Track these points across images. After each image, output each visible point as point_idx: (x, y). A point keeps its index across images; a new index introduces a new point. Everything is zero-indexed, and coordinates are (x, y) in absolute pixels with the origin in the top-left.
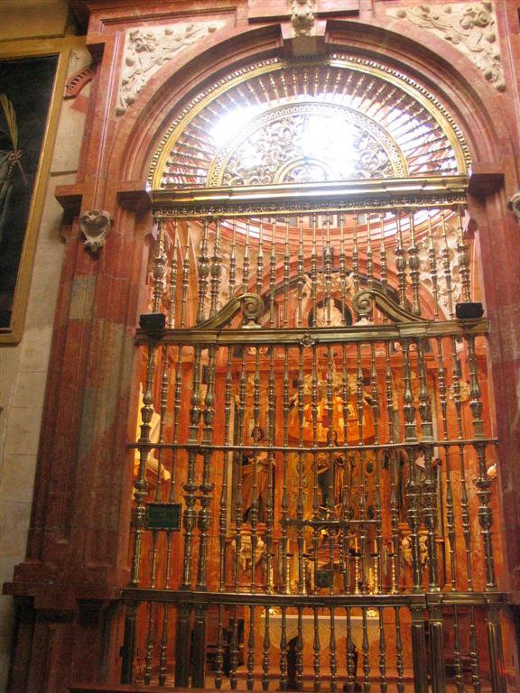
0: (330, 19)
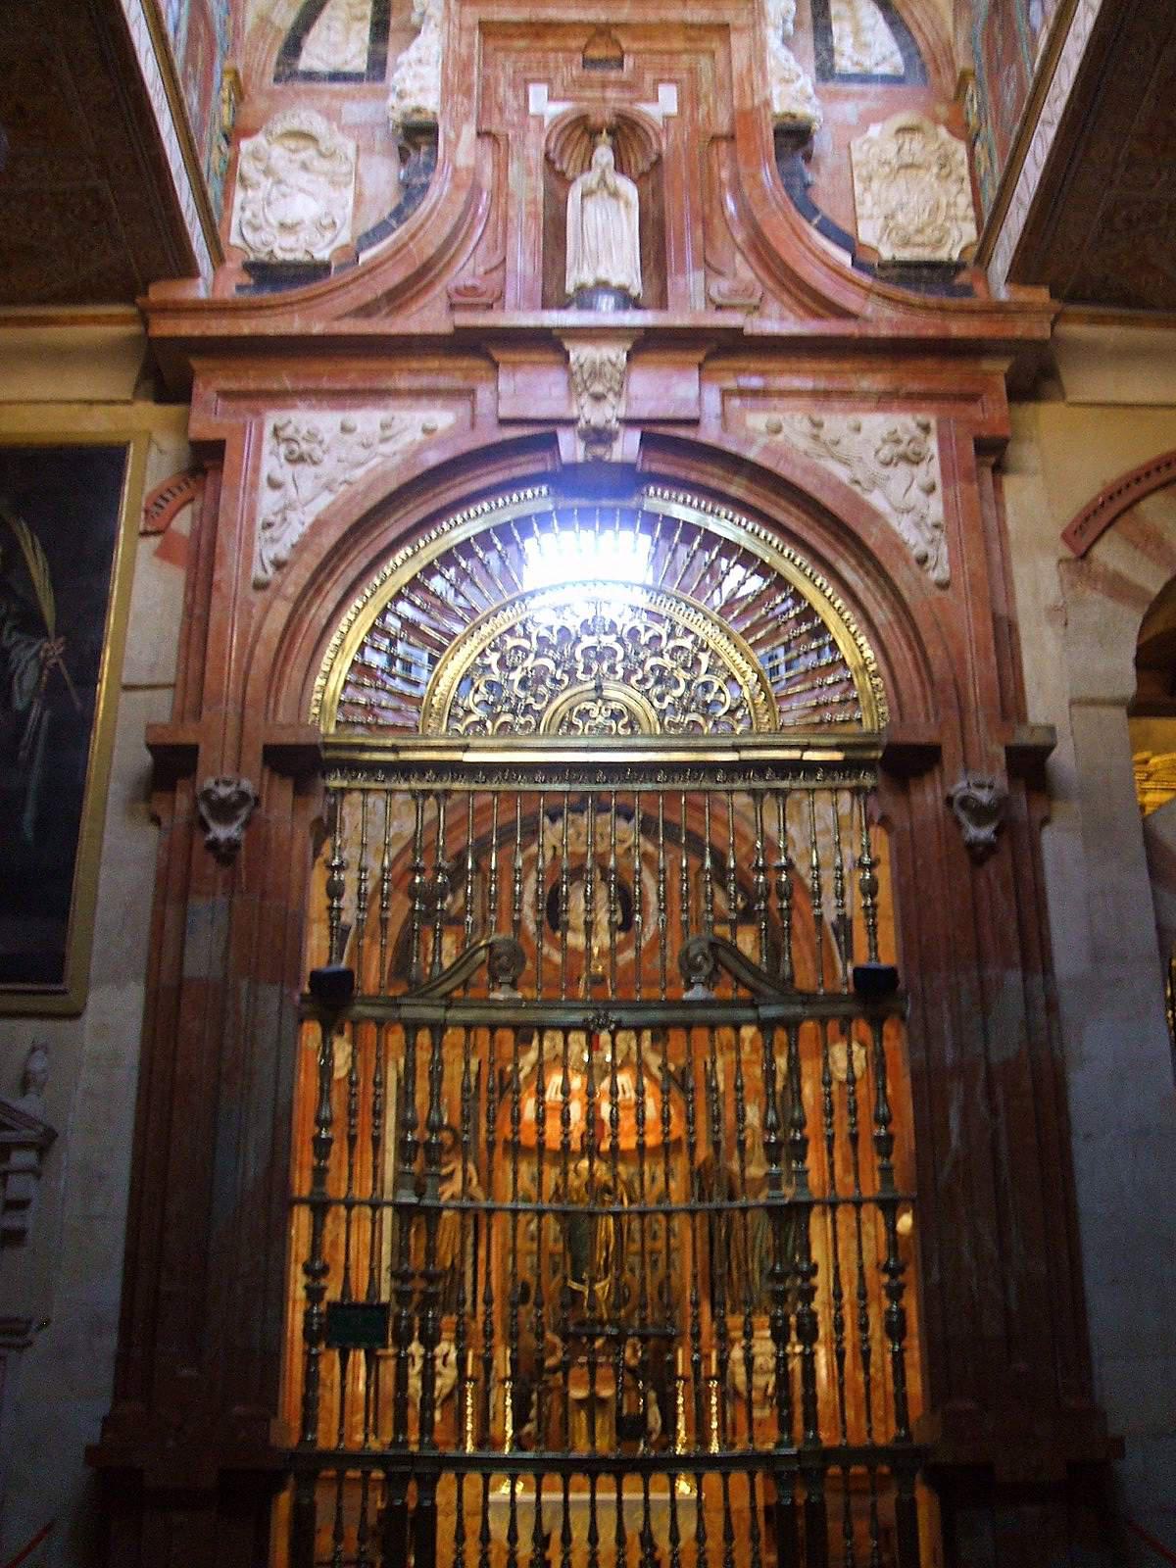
0: (647, 428)
